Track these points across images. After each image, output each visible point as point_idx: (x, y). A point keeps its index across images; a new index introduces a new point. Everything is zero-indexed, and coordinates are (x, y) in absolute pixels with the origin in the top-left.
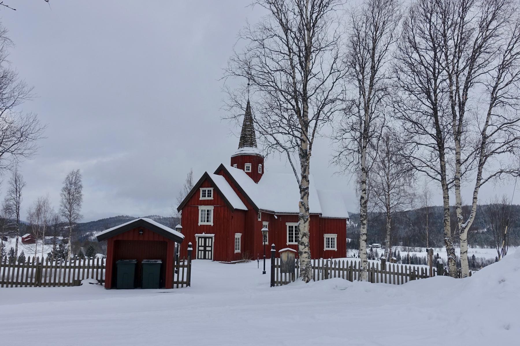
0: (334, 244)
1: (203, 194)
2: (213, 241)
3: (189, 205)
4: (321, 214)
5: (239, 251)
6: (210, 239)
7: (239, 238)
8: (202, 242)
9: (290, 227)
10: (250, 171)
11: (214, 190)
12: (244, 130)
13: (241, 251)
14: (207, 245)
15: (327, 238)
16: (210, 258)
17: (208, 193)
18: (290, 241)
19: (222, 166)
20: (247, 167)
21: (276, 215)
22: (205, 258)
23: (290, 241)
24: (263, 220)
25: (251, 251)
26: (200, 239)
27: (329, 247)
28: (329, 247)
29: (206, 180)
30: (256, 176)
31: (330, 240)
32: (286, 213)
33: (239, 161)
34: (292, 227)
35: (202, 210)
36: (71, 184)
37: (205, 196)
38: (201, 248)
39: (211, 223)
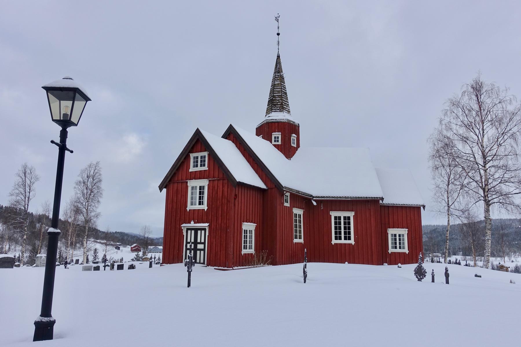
0: (404, 243)
1: (194, 162)
3: (175, 182)
4: (382, 199)
5: (252, 251)
6: (203, 232)
7: (251, 232)
10: (280, 143)
11: (209, 155)
12: (272, 91)
14: (199, 241)
15: (392, 235)
16: (202, 261)
17: (201, 161)
19: (231, 127)
20: (275, 137)
21: (315, 200)
24: (293, 205)
25: (272, 251)
26: (189, 232)
27: (396, 248)
28: (396, 248)
29: (198, 142)
30: (288, 150)
31: (398, 238)
33: (265, 131)
35: (193, 188)
36: (88, 177)
37: (197, 166)
39: (205, 207)
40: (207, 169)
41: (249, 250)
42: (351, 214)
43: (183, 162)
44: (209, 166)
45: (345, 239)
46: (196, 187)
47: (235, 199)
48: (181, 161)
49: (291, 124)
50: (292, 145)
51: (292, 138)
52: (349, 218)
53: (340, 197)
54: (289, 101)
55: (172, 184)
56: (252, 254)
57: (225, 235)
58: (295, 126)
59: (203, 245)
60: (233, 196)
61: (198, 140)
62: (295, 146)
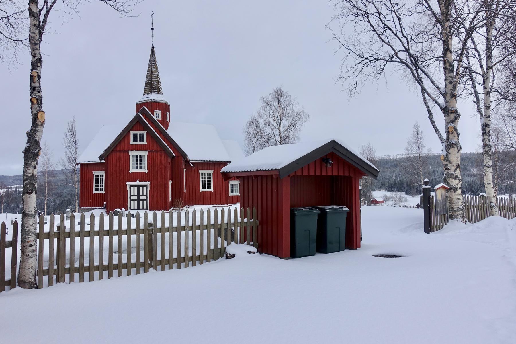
1: (134, 138)
2: (149, 189)
6: (145, 188)
16: (145, 207)
18: (202, 188)
23: (202, 188)
26: (132, 188)
37: (137, 141)
42: (211, 172)
45: (208, 188)
52: (210, 174)
55: (114, 153)
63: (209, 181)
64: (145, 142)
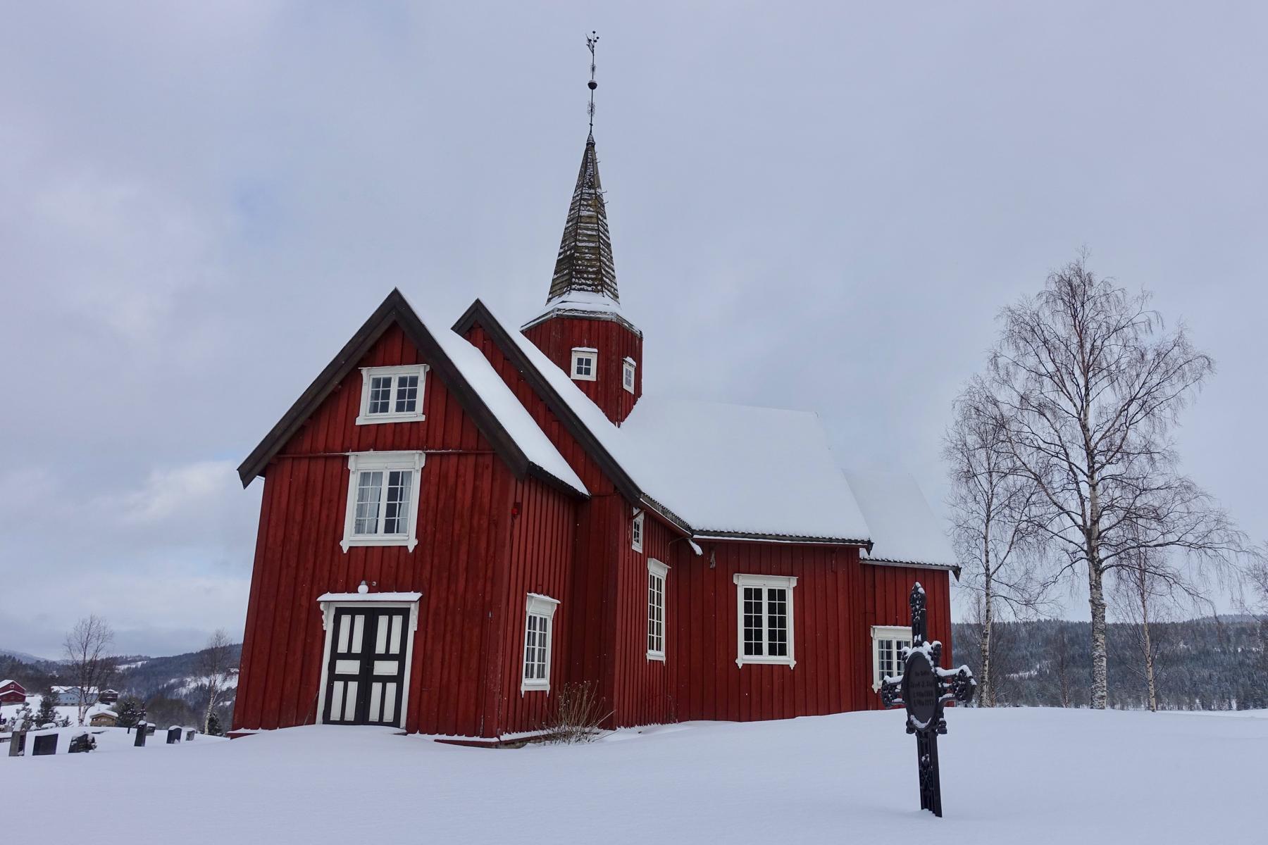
1: (375, 396)
6: (397, 620)
8: (351, 635)
9: (748, 592)
10: (592, 377)
11: (430, 376)
13: (553, 682)
14: (380, 648)
17: (401, 394)
20: (580, 361)
21: (698, 542)
22: (362, 718)
23: (748, 652)
24: (649, 553)
26: (346, 620)
32: (735, 534)
34: (758, 592)
35: (365, 476)
37: (385, 408)
38: (344, 667)
39: (408, 539)
40: (423, 418)
41: (536, 683)
42: (788, 584)
43: (335, 394)
44: (427, 410)
46: (378, 475)
47: (514, 516)
48: (330, 389)
49: (624, 329)
50: (625, 387)
51: (625, 367)
52: (782, 594)
53: (764, 536)
54: (615, 267)
56: (543, 692)
57: (476, 631)
58: (633, 335)
59: (395, 664)
60: (510, 506)
61: (394, 325)
62: (631, 389)
63: (777, 622)
64: (418, 415)
